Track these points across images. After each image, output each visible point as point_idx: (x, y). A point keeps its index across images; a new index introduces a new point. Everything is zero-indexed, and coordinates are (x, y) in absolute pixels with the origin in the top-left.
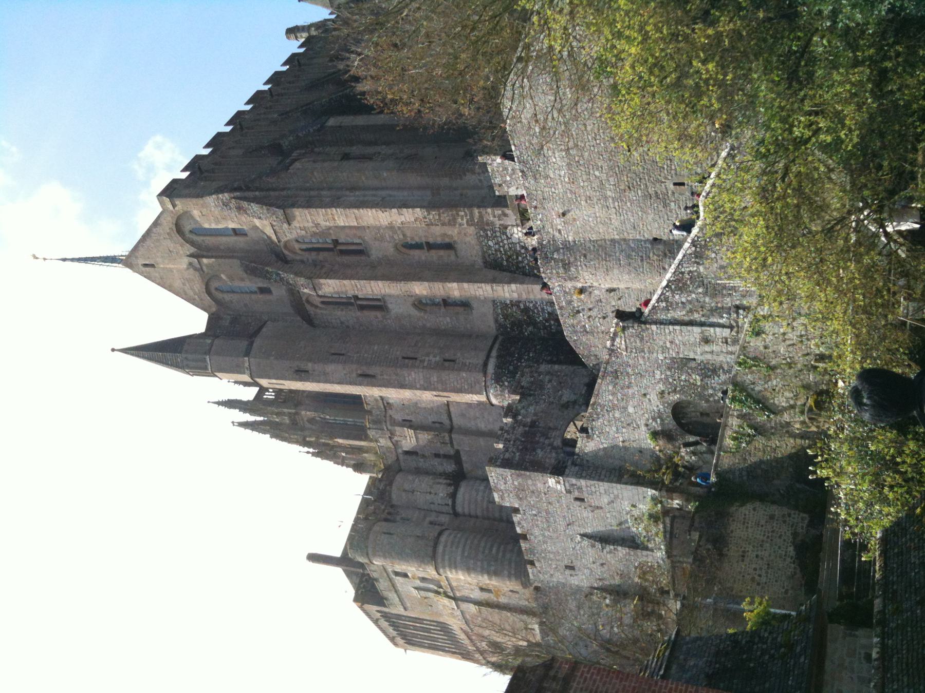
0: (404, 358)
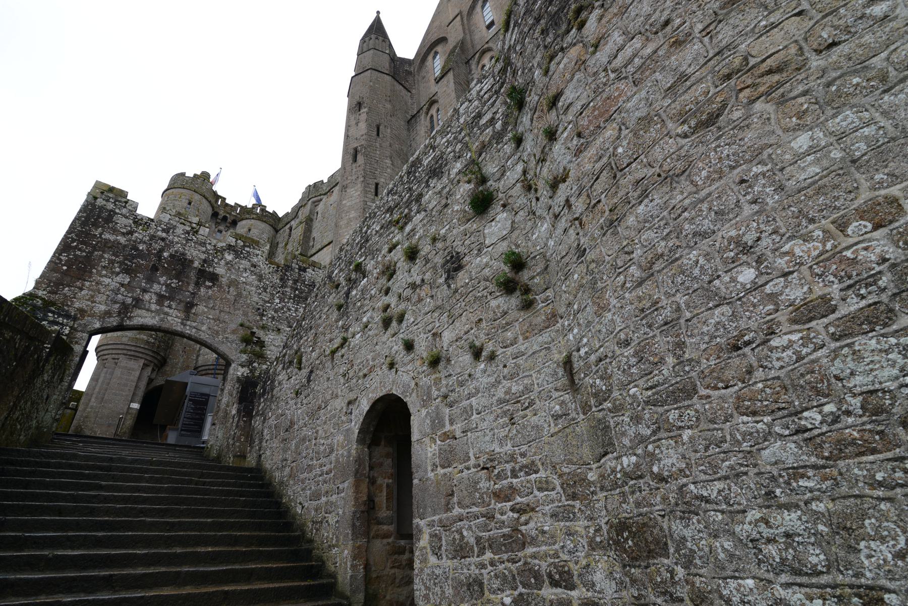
0: (377, 185)
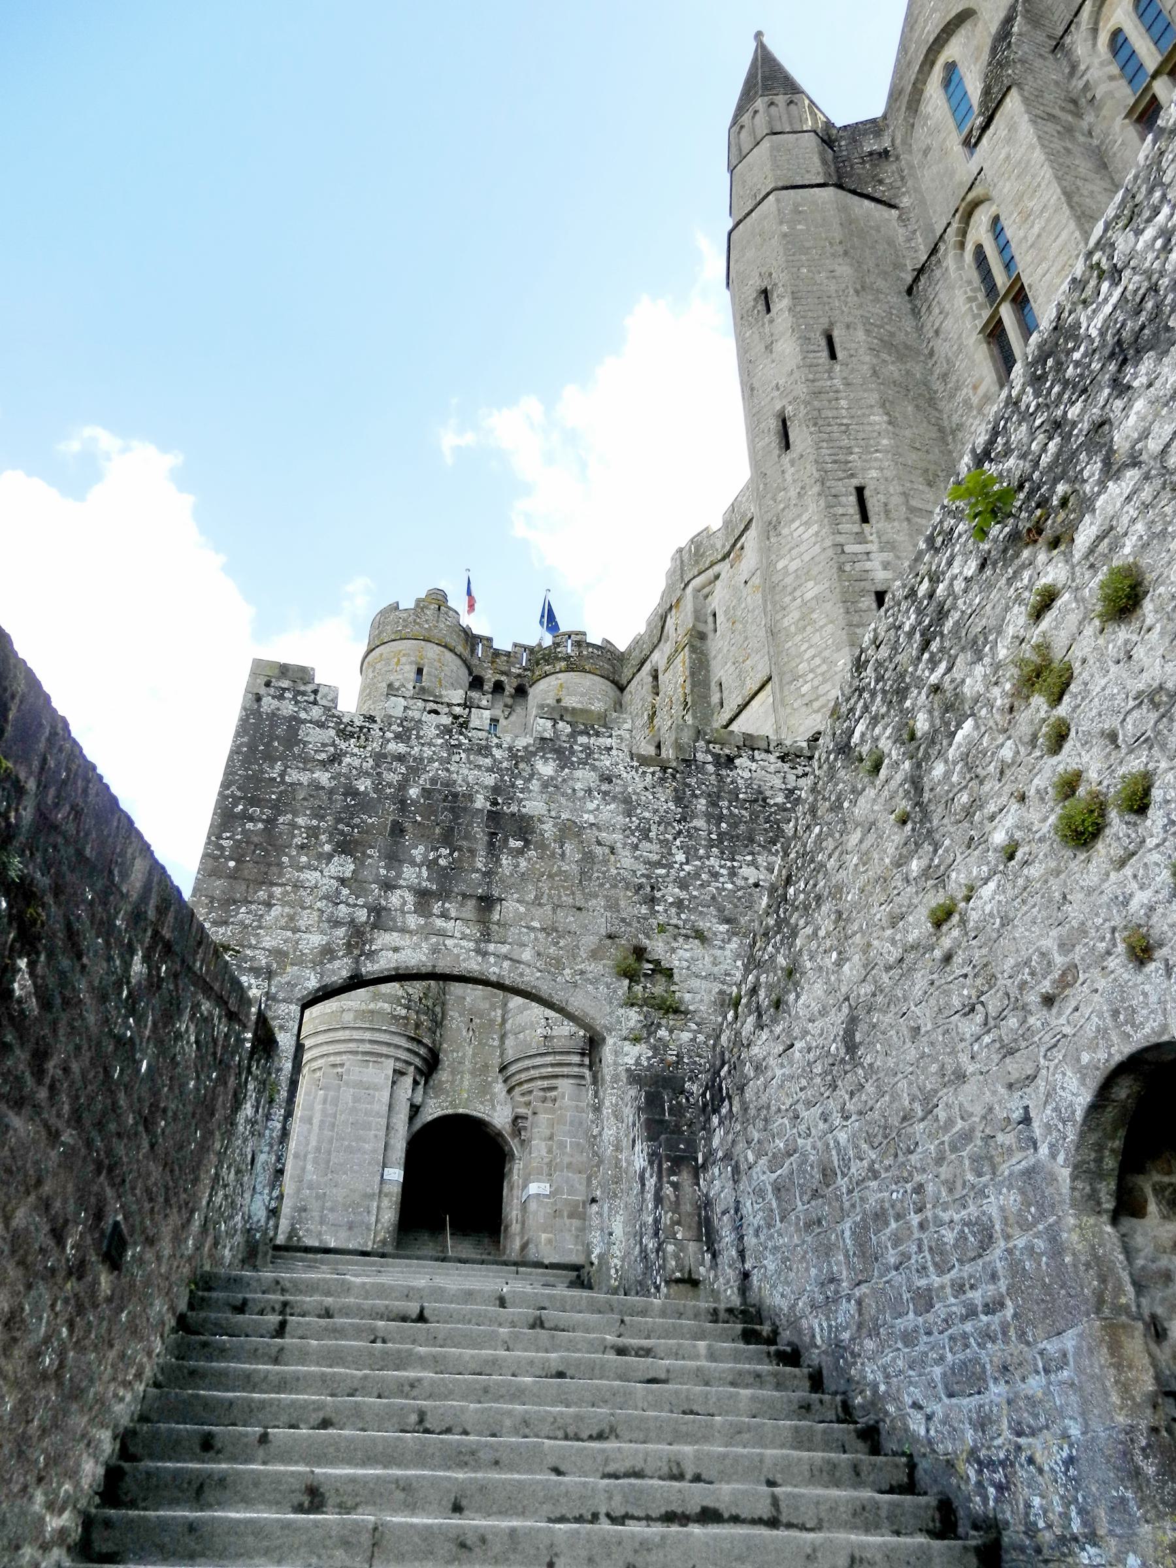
0: (860, 491)
